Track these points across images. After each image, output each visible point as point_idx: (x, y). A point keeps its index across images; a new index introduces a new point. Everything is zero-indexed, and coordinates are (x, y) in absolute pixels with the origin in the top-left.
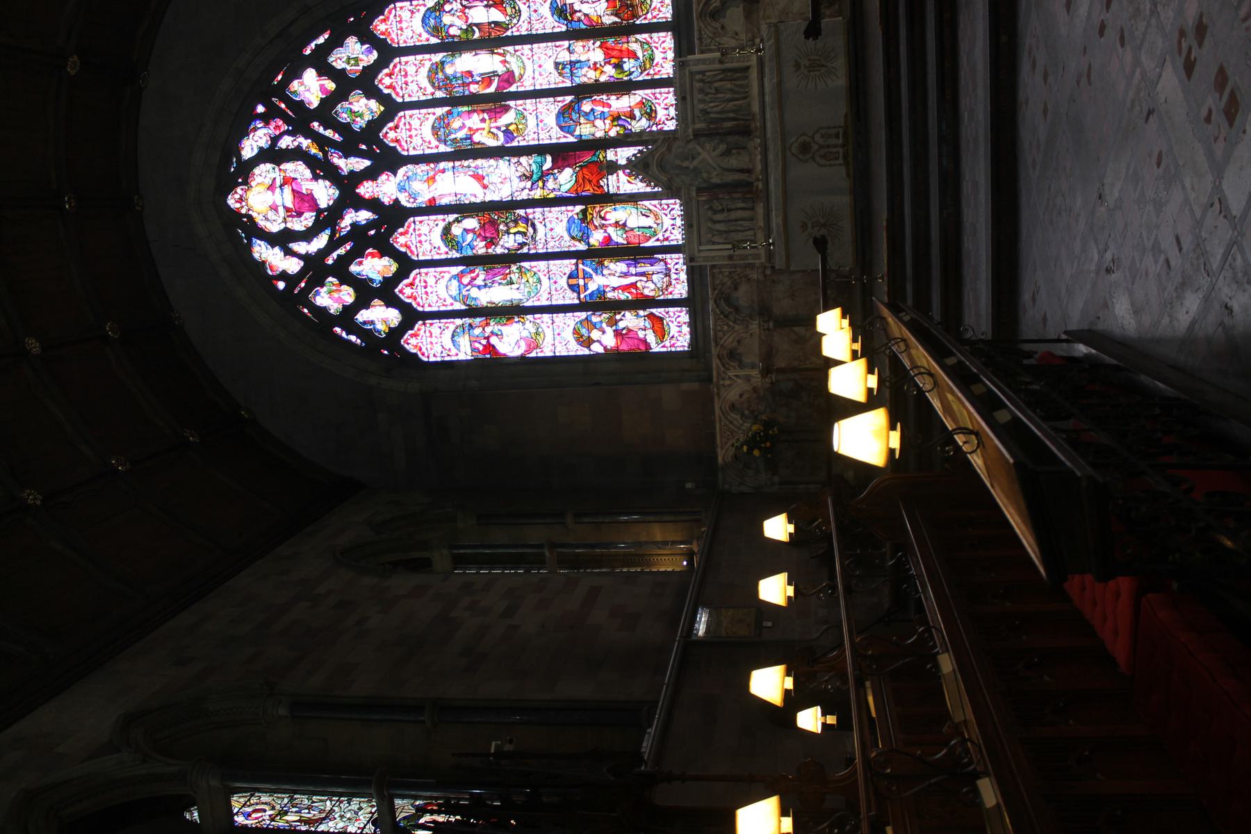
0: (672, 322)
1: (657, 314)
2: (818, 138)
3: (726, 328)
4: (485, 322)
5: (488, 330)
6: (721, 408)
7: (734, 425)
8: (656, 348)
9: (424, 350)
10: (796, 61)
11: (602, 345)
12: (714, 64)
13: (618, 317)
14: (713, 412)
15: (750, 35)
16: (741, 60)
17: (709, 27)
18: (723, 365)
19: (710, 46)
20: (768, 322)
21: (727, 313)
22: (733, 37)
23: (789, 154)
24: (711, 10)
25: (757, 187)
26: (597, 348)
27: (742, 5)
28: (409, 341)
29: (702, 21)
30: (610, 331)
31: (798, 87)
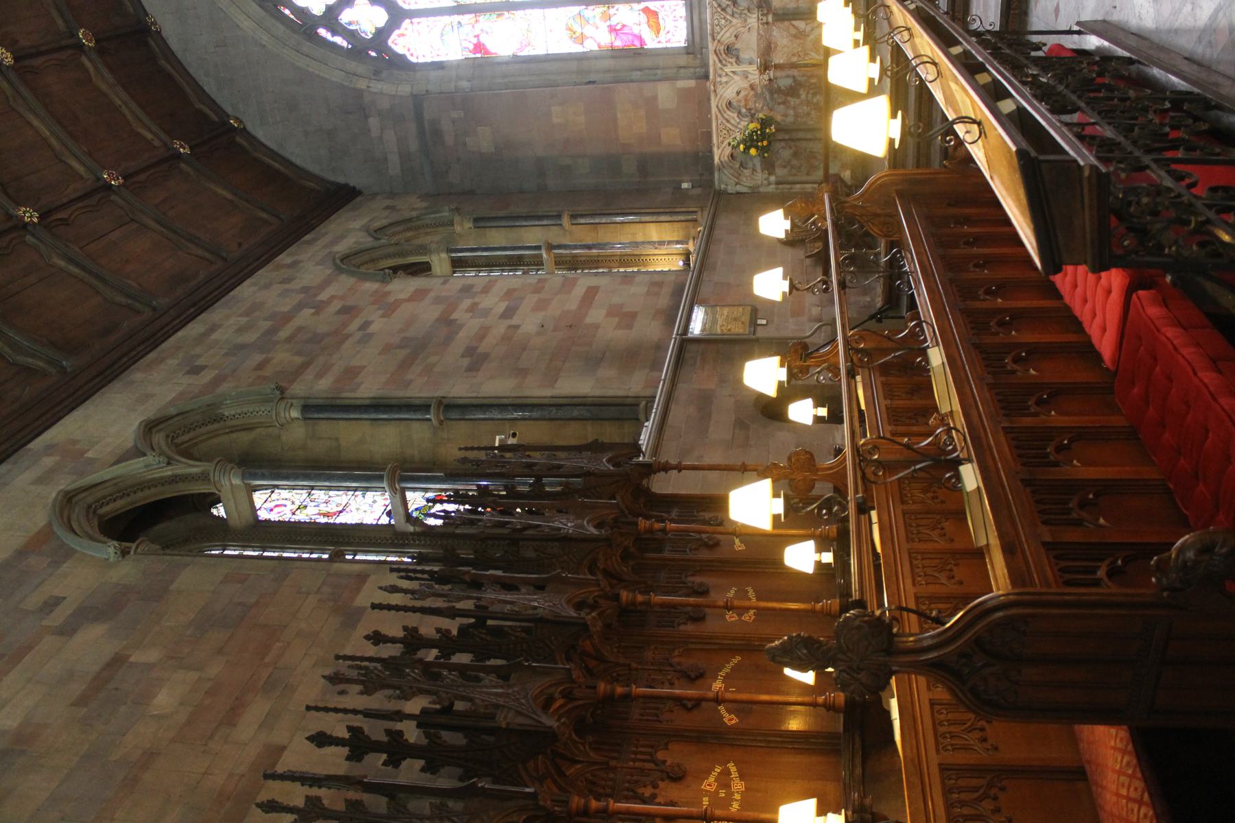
0: (668, 16)
1: (653, 8)
3: (723, 22)
4: (474, 19)
5: (478, 27)
6: (717, 106)
7: (732, 125)
8: (651, 43)
9: (412, 51)
11: (596, 41)
13: (612, 11)
14: (710, 112)
18: (720, 61)
20: (766, 15)
21: (724, 6)
26: (590, 46)
28: (396, 42)
30: (604, 27)
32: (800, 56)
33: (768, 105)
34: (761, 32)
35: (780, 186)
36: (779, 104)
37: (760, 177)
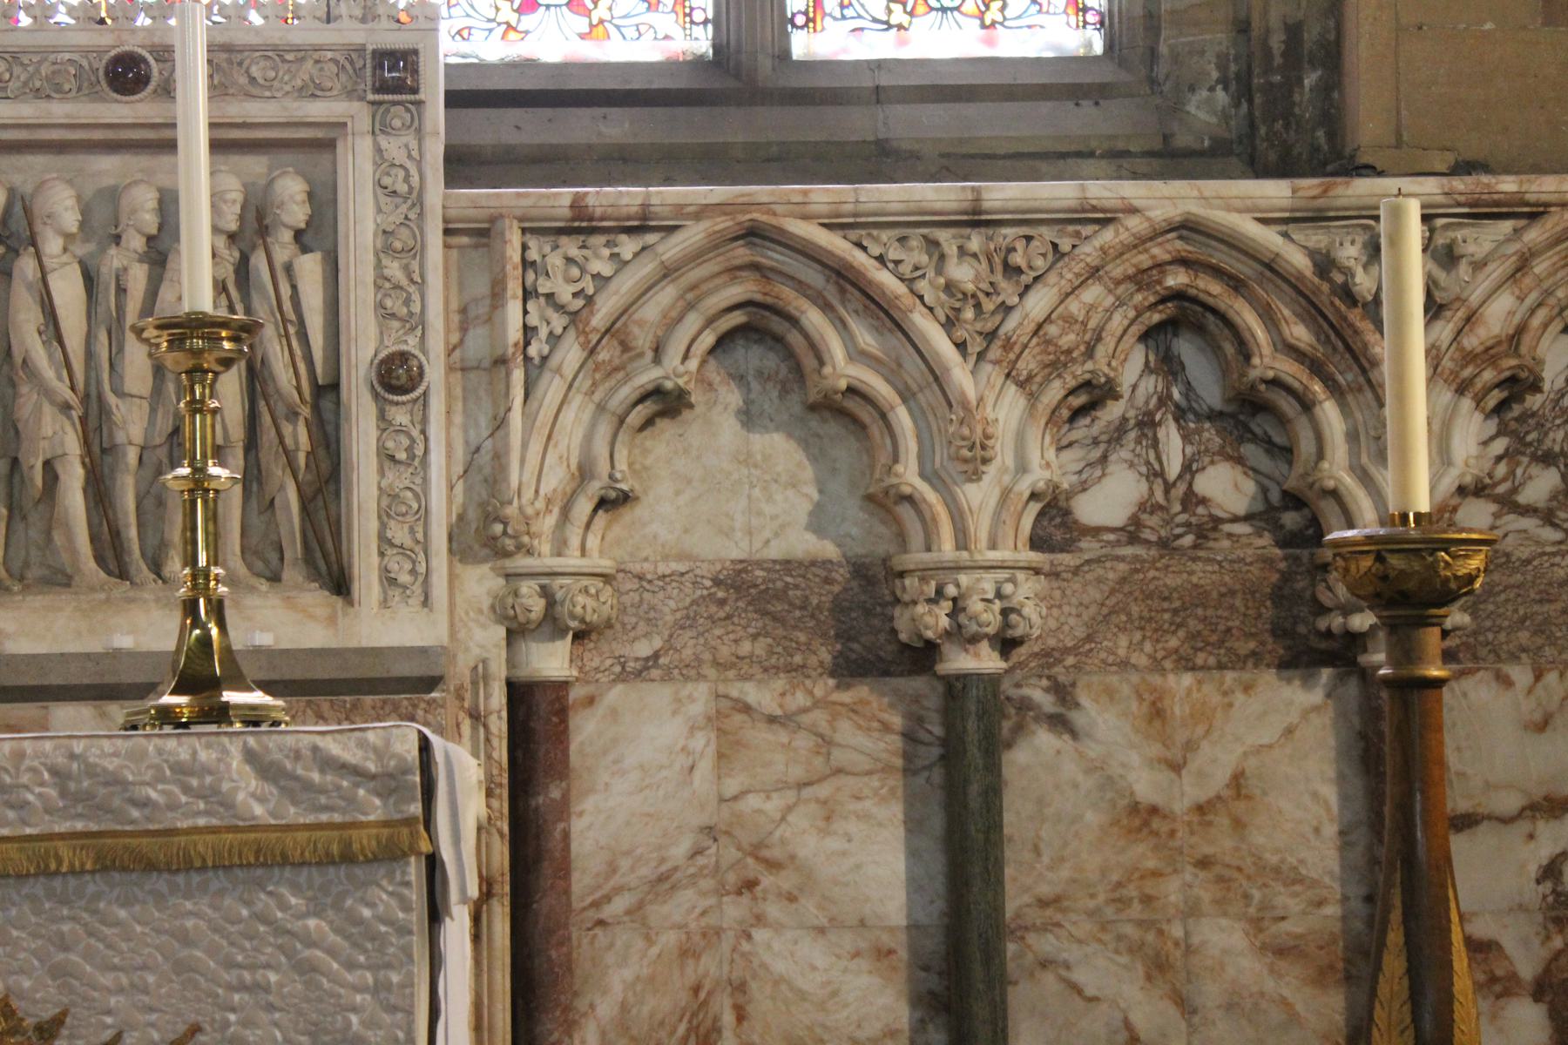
12: (385, 314)
15: (585, 604)
16: (399, 533)
17: (666, 296)
19: (527, 294)
22: (584, 473)
24: (794, 321)
27: (829, 550)
29: (717, 244)
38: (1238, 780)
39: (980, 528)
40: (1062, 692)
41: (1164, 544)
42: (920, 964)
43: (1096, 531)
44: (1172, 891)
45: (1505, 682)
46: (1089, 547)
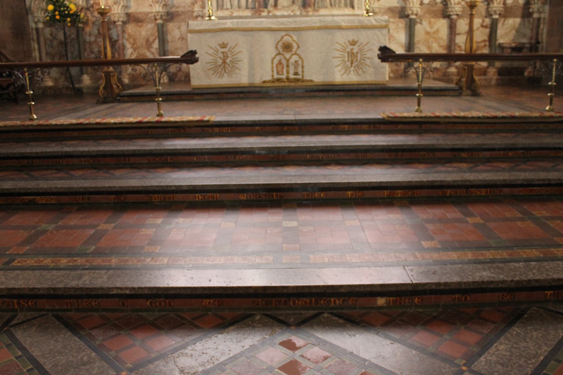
2: (295, 58)
10: (357, 42)
15: (377, 10)
16: (360, 3)
20: (161, 18)
23: (283, 33)
25: (263, 11)
31: (337, 43)
32: (134, 44)
33: (96, 21)
34: (150, 15)
35: (34, 32)
36: (98, 30)
37: (40, 15)
38: (438, 30)
39: (415, 3)
40: (421, 20)
41: (432, 5)
42: (406, 47)
43: (425, 4)
44: (431, 40)
45: (464, 20)
46: (424, 5)
